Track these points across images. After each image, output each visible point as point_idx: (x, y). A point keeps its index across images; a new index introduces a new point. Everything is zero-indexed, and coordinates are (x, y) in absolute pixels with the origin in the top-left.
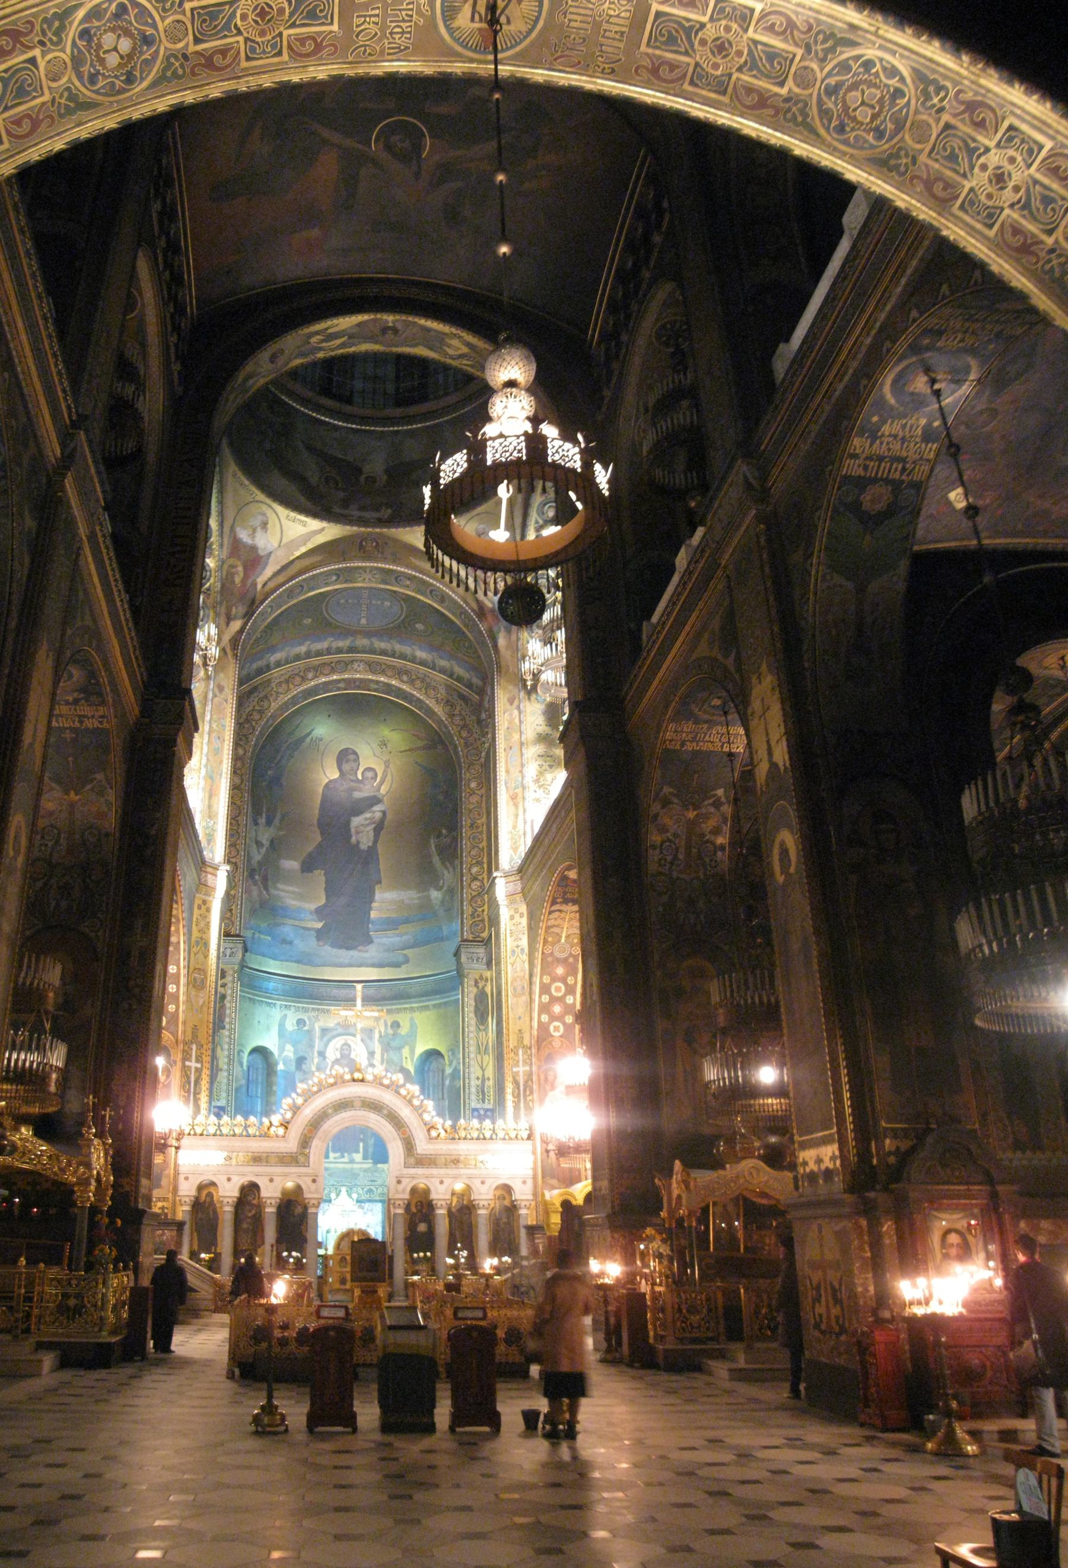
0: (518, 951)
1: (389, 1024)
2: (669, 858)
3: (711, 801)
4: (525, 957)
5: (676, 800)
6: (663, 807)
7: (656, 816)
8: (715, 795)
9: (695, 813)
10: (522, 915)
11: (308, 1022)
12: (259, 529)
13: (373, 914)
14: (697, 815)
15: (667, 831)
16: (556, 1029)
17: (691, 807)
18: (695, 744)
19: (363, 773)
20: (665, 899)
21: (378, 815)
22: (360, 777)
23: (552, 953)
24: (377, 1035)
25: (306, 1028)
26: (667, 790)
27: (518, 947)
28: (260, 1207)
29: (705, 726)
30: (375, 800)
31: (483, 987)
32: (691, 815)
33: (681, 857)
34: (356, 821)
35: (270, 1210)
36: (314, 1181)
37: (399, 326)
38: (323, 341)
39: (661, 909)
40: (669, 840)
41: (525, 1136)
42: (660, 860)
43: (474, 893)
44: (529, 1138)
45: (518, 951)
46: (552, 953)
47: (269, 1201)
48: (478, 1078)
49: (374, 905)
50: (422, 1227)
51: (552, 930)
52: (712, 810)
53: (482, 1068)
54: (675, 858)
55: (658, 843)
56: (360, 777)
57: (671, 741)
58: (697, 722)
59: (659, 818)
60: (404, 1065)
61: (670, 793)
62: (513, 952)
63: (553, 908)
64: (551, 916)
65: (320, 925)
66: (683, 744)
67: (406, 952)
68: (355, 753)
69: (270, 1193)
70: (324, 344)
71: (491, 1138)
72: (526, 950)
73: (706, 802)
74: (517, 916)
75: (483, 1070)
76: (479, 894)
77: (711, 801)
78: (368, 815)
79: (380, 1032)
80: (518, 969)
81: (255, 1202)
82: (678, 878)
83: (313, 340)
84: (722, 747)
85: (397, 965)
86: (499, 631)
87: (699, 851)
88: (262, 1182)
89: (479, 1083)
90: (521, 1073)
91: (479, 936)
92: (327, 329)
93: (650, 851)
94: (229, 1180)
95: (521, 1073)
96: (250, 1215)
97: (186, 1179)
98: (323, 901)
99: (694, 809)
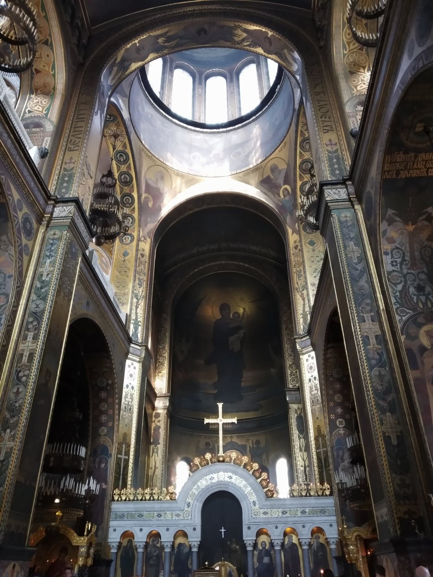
0: (312, 379)
1: (254, 442)
2: (399, 260)
3: (424, 217)
4: (317, 382)
5: (397, 219)
6: (389, 225)
7: (385, 232)
8: (427, 212)
9: (414, 227)
10: (312, 358)
11: (211, 444)
12: (159, 179)
13: (243, 384)
14: (414, 229)
15: (394, 242)
16: (341, 423)
17: (410, 223)
18: (407, 172)
19: (233, 315)
20: (400, 287)
21: (242, 335)
22: (231, 317)
23: (332, 375)
24: (248, 449)
25: (210, 447)
26: (390, 212)
27: (312, 376)
28: (162, 548)
29: (413, 154)
30: (239, 328)
31: (300, 413)
32: (411, 228)
33: (407, 258)
34: (231, 339)
35: (168, 550)
36: (194, 529)
37: (206, 27)
38: (165, 42)
39: (398, 294)
40: (397, 248)
41: (328, 492)
42: (392, 262)
43: (290, 363)
44: (331, 494)
45: (312, 379)
46: (332, 375)
47: (165, 544)
48: (302, 466)
49: (243, 379)
50: (266, 560)
51: (330, 360)
52: (426, 223)
53: (303, 460)
54: (403, 260)
55: (389, 251)
56: (231, 317)
57: (388, 171)
58: (406, 152)
59: (388, 232)
60: (264, 465)
61: (393, 214)
62: (310, 380)
63: (329, 346)
64: (328, 351)
65: (215, 392)
66: (398, 173)
67: (260, 403)
68: (229, 306)
69: (167, 538)
70: (167, 44)
71: (306, 496)
72: (317, 378)
73: (421, 218)
74: (310, 359)
75: (305, 461)
76: (293, 363)
77: (424, 217)
78: (237, 335)
79: (250, 447)
80: (314, 389)
81: (158, 545)
82: (408, 273)
83: (160, 40)
84: (427, 172)
85: (256, 410)
86: (287, 215)
87: (421, 253)
88: (162, 531)
89: (302, 469)
90: (322, 452)
91: (295, 386)
92: (167, 33)
93: (384, 257)
94: (141, 530)
95: (322, 452)
96: (155, 554)
97: (115, 530)
98: (216, 379)
99: (412, 225)
